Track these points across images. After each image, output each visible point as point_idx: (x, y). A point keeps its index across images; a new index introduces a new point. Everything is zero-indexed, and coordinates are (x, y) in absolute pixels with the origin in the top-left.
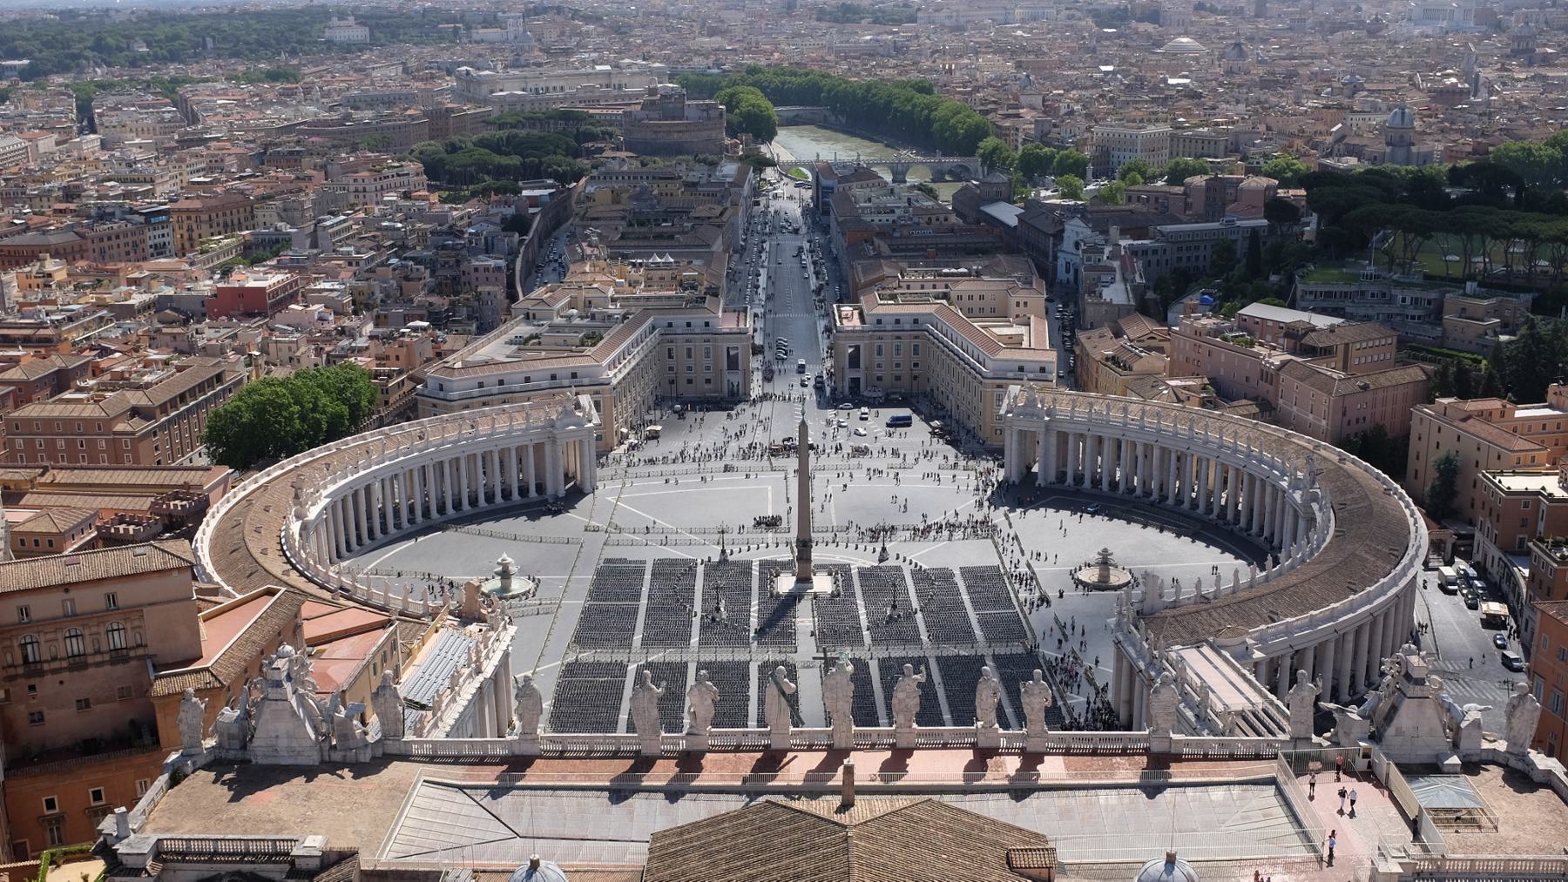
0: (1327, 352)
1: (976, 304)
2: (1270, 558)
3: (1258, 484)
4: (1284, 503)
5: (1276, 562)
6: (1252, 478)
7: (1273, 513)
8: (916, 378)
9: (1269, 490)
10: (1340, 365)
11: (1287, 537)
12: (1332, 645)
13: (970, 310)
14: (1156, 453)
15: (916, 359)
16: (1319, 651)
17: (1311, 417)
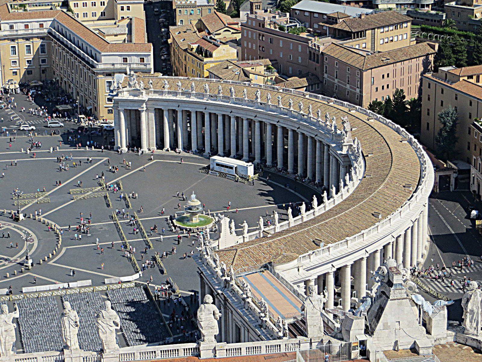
0: (361, 34)
1: (90, 9)
2: (315, 199)
3: (309, 140)
4: (329, 155)
5: (320, 202)
6: (305, 138)
7: (321, 163)
8: (43, 72)
9: (318, 144)
10: (369, 45)
11: (332, 179)
12: (364, 263)
13: (85, 15)
14: (233, 120)
15: (43, 56)
16: (356, 266)
17: (348, 86)
